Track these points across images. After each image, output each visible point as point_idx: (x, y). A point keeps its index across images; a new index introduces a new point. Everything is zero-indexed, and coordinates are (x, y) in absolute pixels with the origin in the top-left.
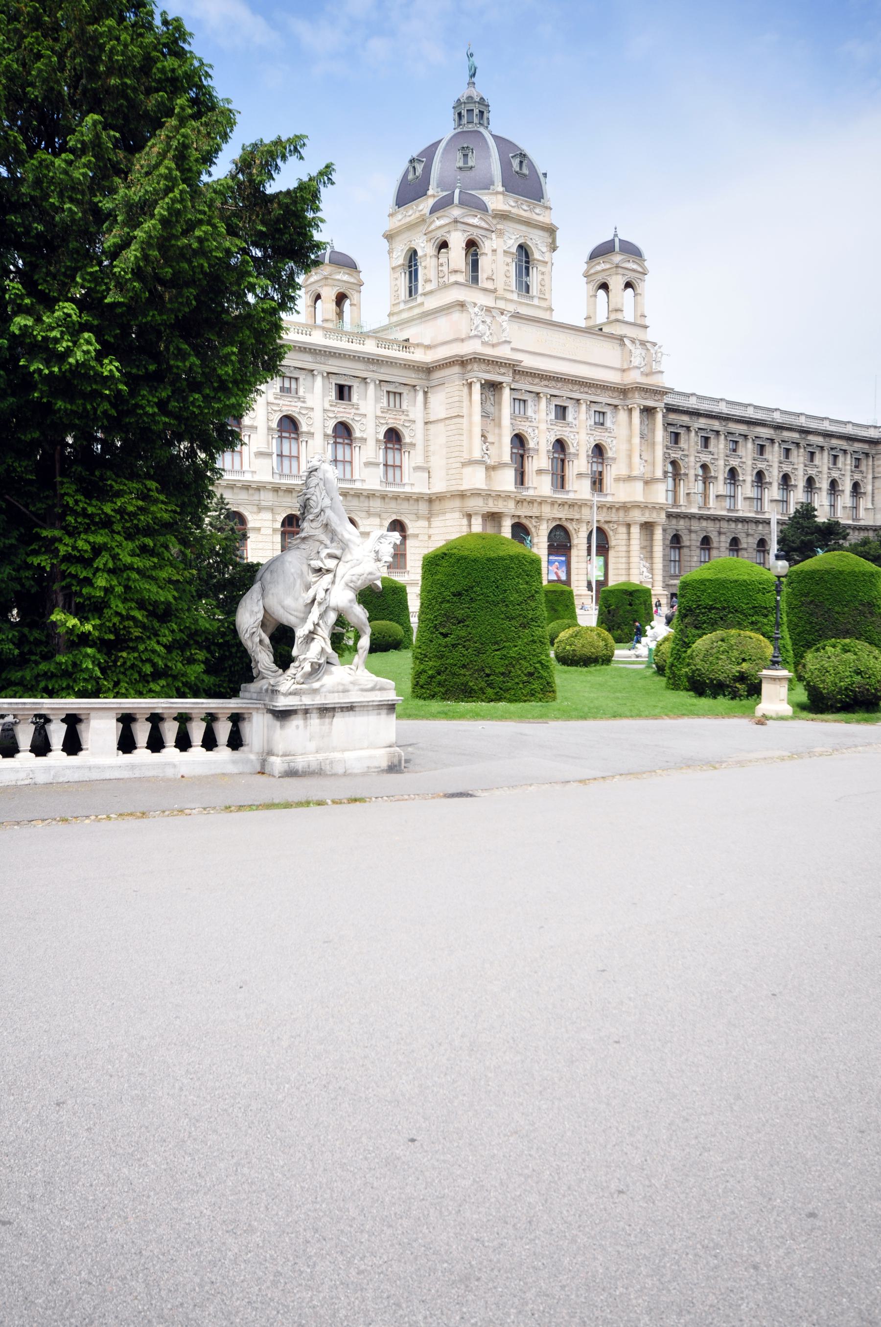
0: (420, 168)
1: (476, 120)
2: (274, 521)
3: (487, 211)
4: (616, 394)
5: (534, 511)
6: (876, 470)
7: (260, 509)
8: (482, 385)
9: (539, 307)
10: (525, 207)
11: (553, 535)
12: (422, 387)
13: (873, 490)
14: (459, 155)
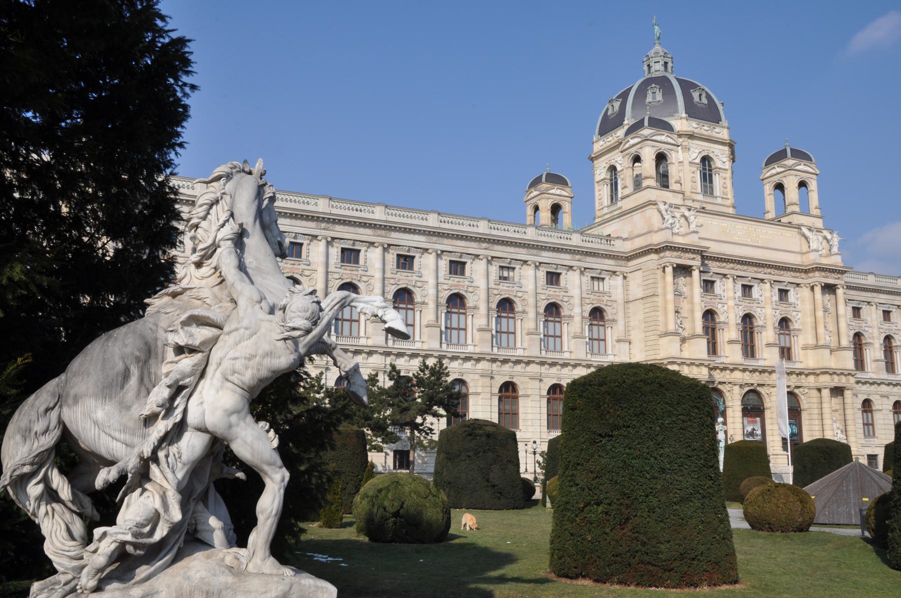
3: (673, 131)
8: (673, 268)
10: (706, 128)
11: (746, 398)
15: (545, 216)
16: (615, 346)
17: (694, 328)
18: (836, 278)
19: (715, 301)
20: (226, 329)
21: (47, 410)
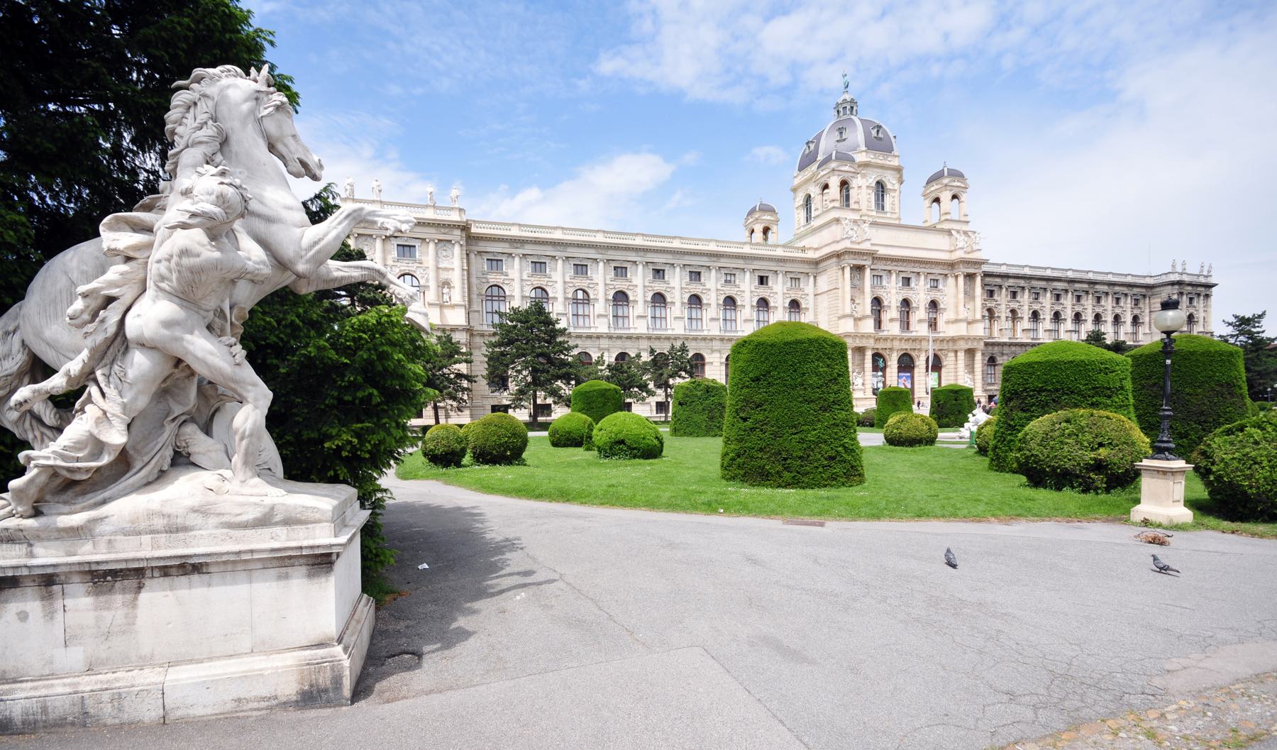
0: (812, 146)
1: (848, 112)
2: (721, 358)
4: (946, 267)
5: (888, 345)
6: (1153, 306)
7: (713, 351)
8: (851, 268)
9: (891, 218)
12: (812, 273)
13: (1150, 320)
14: (837, 133)
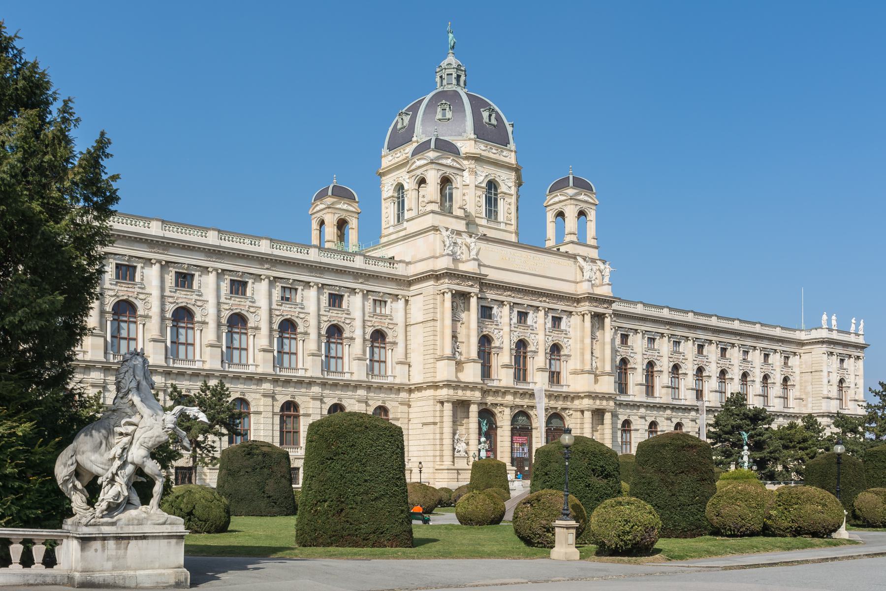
1: (454, 82)
8: (453, 295)
15: (330, 231)
16: (395, 367)
17: (468, 353)
18: (606, 308)
19: (491, 326)
20: (140, 426)
21: (72, 456)
